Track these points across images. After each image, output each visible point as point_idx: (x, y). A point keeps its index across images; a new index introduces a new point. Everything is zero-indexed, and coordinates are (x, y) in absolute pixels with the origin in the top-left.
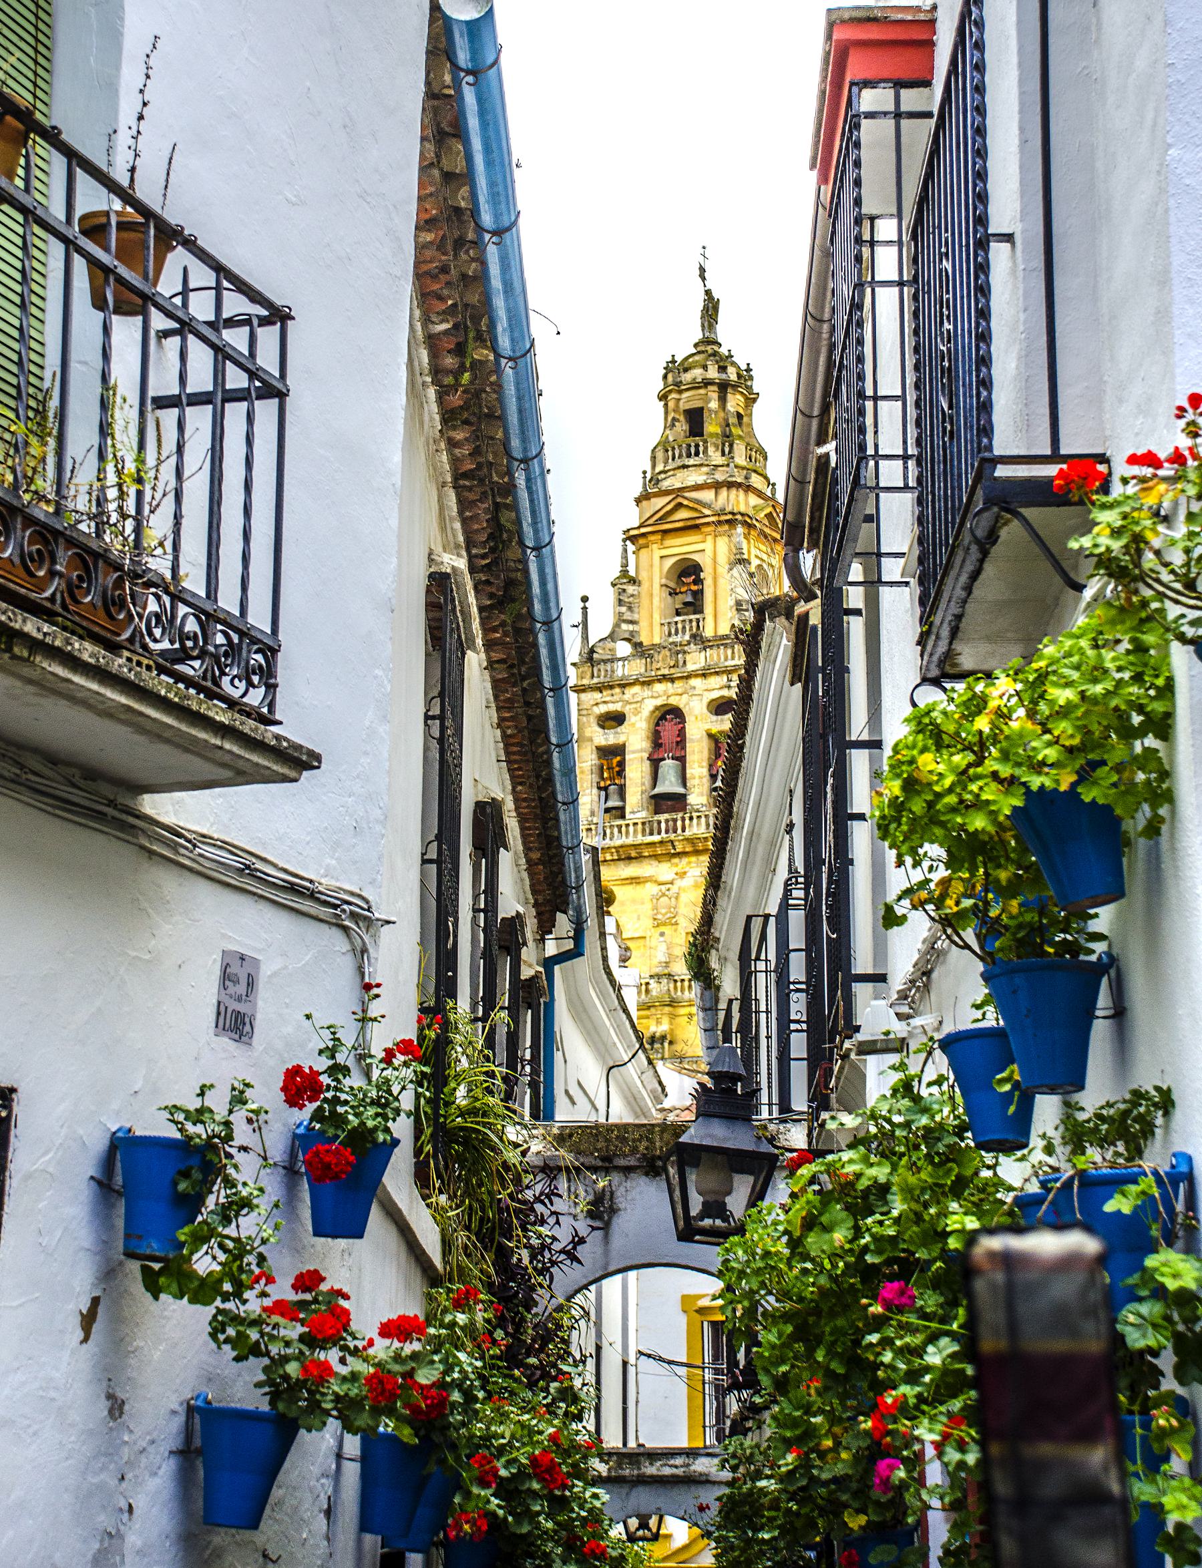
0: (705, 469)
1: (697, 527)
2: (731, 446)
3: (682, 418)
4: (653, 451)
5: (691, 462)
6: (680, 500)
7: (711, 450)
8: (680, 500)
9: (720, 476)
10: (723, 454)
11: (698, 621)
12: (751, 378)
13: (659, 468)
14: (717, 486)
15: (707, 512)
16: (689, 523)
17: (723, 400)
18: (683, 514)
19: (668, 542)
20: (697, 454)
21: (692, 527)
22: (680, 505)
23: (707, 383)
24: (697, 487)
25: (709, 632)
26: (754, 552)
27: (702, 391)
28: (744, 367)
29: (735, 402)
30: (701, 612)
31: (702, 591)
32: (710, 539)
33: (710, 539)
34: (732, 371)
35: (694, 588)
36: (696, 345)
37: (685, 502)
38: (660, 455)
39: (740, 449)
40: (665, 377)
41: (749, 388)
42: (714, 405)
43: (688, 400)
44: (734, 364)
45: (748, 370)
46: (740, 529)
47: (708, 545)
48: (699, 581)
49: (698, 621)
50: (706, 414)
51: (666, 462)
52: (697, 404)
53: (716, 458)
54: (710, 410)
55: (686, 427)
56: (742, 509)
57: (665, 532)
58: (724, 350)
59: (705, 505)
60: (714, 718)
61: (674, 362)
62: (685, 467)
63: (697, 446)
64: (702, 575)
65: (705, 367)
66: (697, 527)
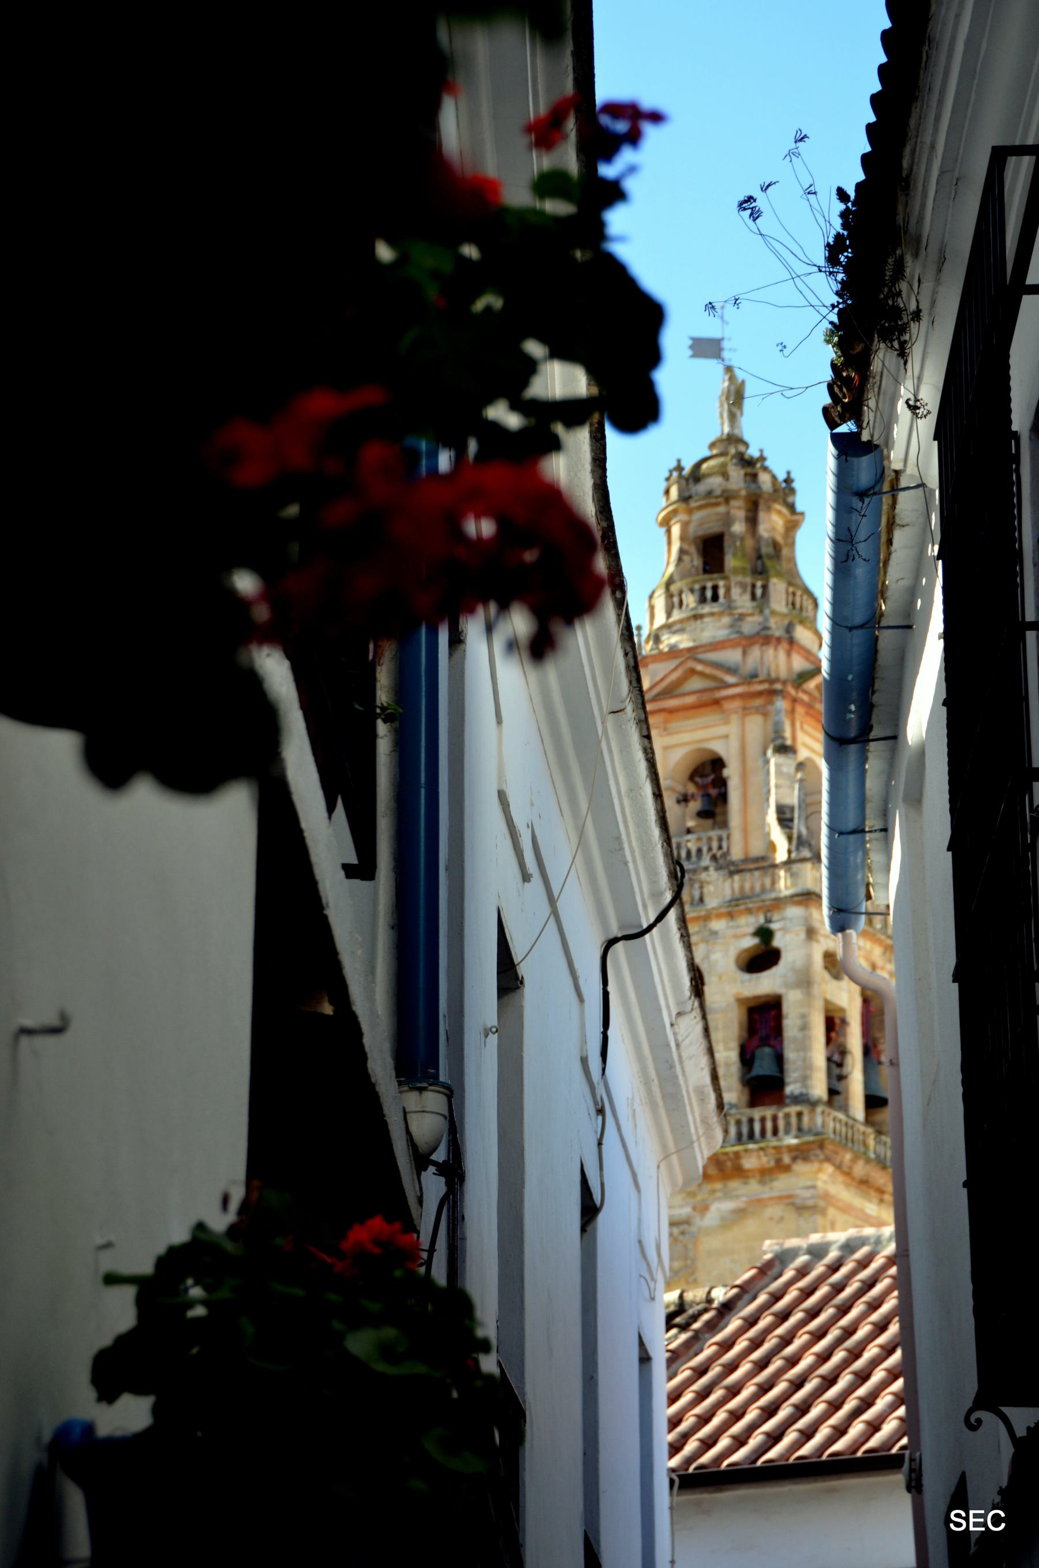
0: (726, 620)
1: (717, 702)
2: (765, 587)
3: (693, 550)
4: (651, 597)
5: (707, 609)
6: (691, 664)
7: (735, 592)
8: (691, 664)
9: (750, 626)
10: (753, 597)
11: (720, 840)
12: (792, 491)
13: (660, 619)
14: (747, 642)
15: (730, 679)
16: (706, 697)
17: (752, 521)
18: (695, 684)
19: (673, 726)
20: (715, 598)
21: (711, 703)
22: (693, 672)
23: (727, 497)
24: (716, 646)
25: (736, 853)
26: (802, 738)
27: (722, 509)
28: (781, 476)
29: (772, 522)
30: (724, 824)
31: (724, 798)
32: (735, 718)
33: (735, 718)
34: (764, 478)
35: (713, 792)
36: (712, 446)
37: (699, 667)
38: (660, 603)
39: (778, 587)
40: (667, 492)
41: (792, 507)
42: (739, 528)
43: (706, 520)
44: (765, 469)
45: (788, 480)
46: (781, 704)
47: (732, 729)
48: (721, 783)
49: (720, 840)
50: (727, 542)
51: (669, 614)
52: (714, 528)
53: (742, 601)
54: (733, 536)
55: (698, 562)
56: (783, 674)
57: (671, 711)
58: (753, 452)
59: (731, 670)
60: (747, 976)
61: (679, 468)
62: (697, 617)
63: (715, 588)
64: (726, 772)
65: (725, 475)
66: (717, 702)
